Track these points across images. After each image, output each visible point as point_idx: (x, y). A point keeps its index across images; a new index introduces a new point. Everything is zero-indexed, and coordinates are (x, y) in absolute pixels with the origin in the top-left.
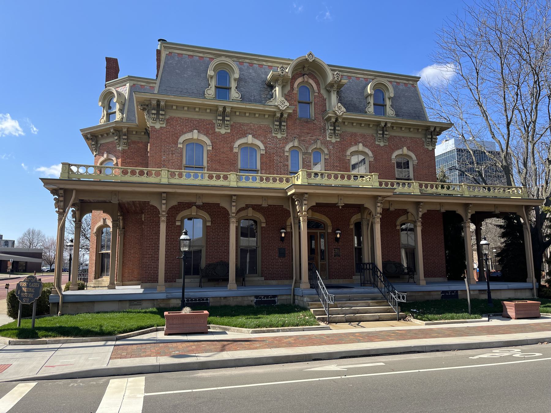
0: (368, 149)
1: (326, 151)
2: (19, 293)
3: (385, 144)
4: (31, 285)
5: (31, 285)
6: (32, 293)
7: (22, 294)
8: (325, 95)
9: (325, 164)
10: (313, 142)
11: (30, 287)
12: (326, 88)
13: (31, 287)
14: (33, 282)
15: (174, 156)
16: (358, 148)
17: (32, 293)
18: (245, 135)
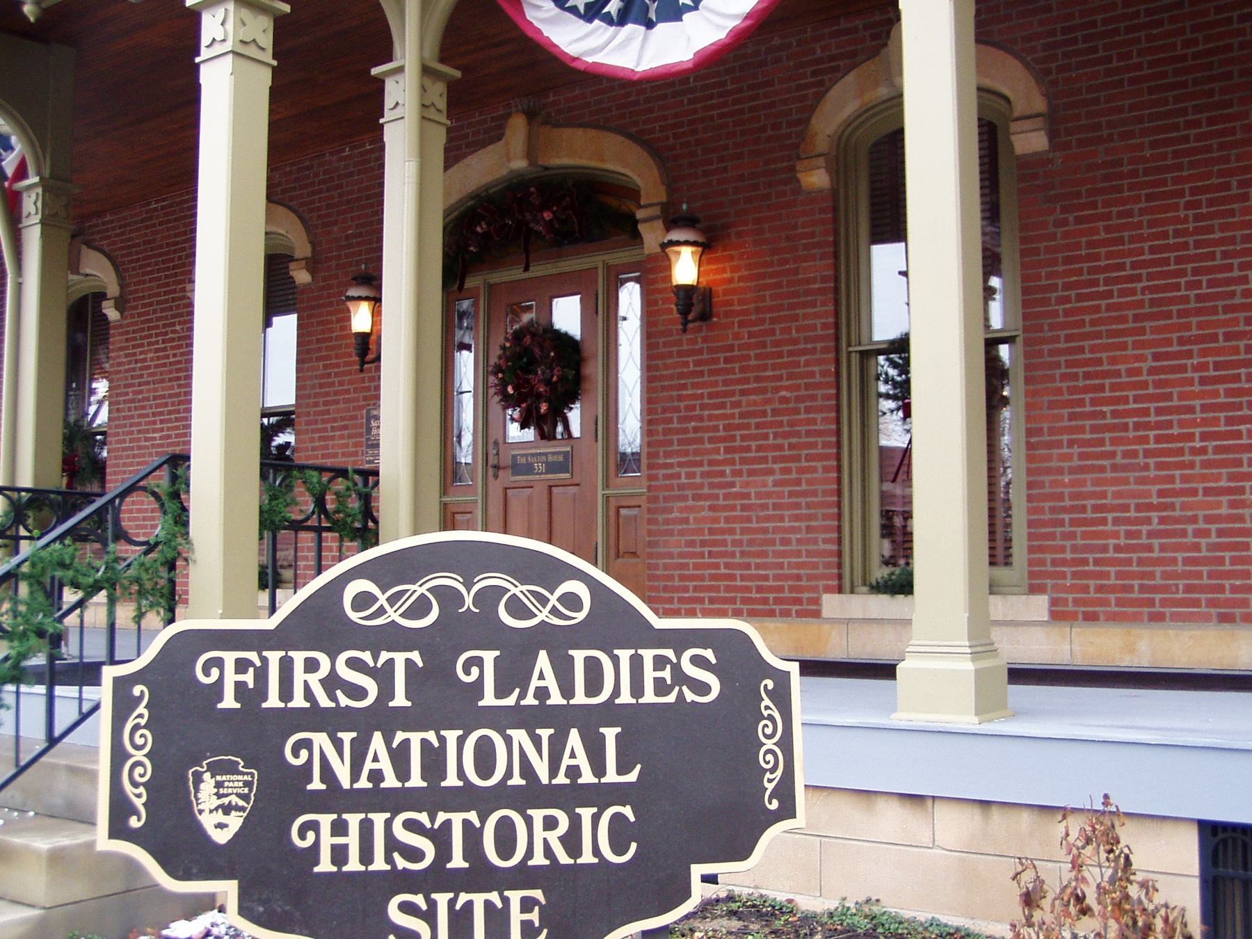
6: (601, 796)
11: (502, 719)
13: (528, 719)
17: (601, 796)
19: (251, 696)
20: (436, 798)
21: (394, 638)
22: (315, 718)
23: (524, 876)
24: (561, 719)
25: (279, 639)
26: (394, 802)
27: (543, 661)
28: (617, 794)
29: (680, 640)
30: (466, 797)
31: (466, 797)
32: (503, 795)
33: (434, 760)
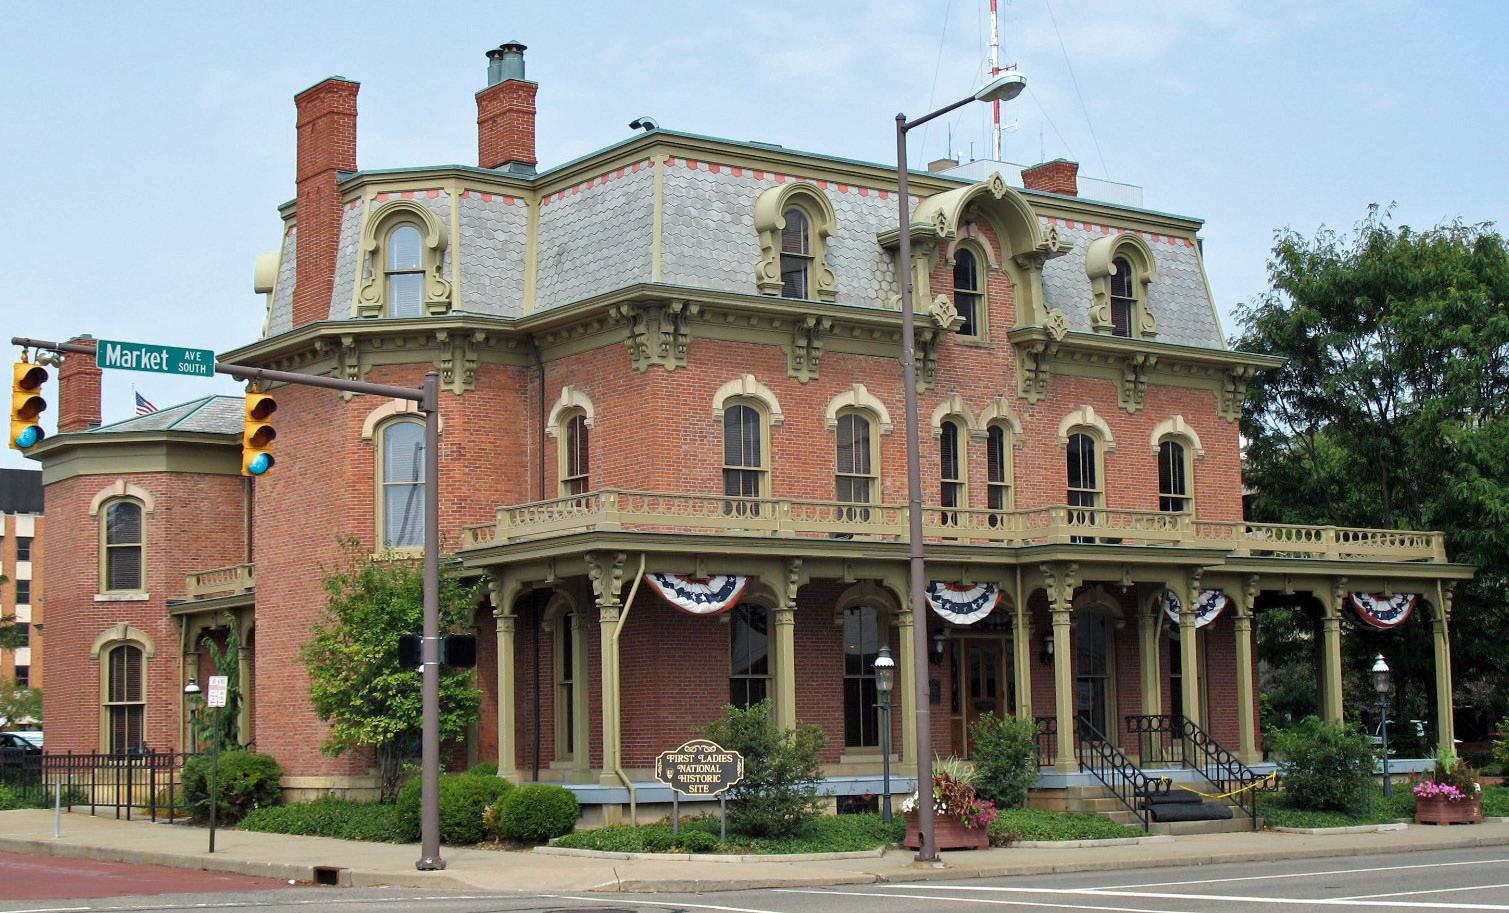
0: (1102, 421)
1: (1018, 428)
2: (670, 776)
3: (1138, 407)
4: (706, 758)
5: (706, 758)
7: (681, 778)
8: (1014, 277)
9: (1014, 459)
10: (989, 401)
12: (1014, 259)
14: (711, 754)
15: (705, 442)
16: (1084, 417)
17: (716, 774)
18: (846, 384)
19: (673, 761)
20: (695, 773)
21: (691, 753)
22: (681, 763)
23: (706, 783)
24: (711, 764)
25: (677, 754)
26: (691, 774)
27: (709, 757)
28: (718, 773)
29: (727, 754)
30: (699, 773)
31: (699, 773)
32: (704, 773)
33: (695, 769)
